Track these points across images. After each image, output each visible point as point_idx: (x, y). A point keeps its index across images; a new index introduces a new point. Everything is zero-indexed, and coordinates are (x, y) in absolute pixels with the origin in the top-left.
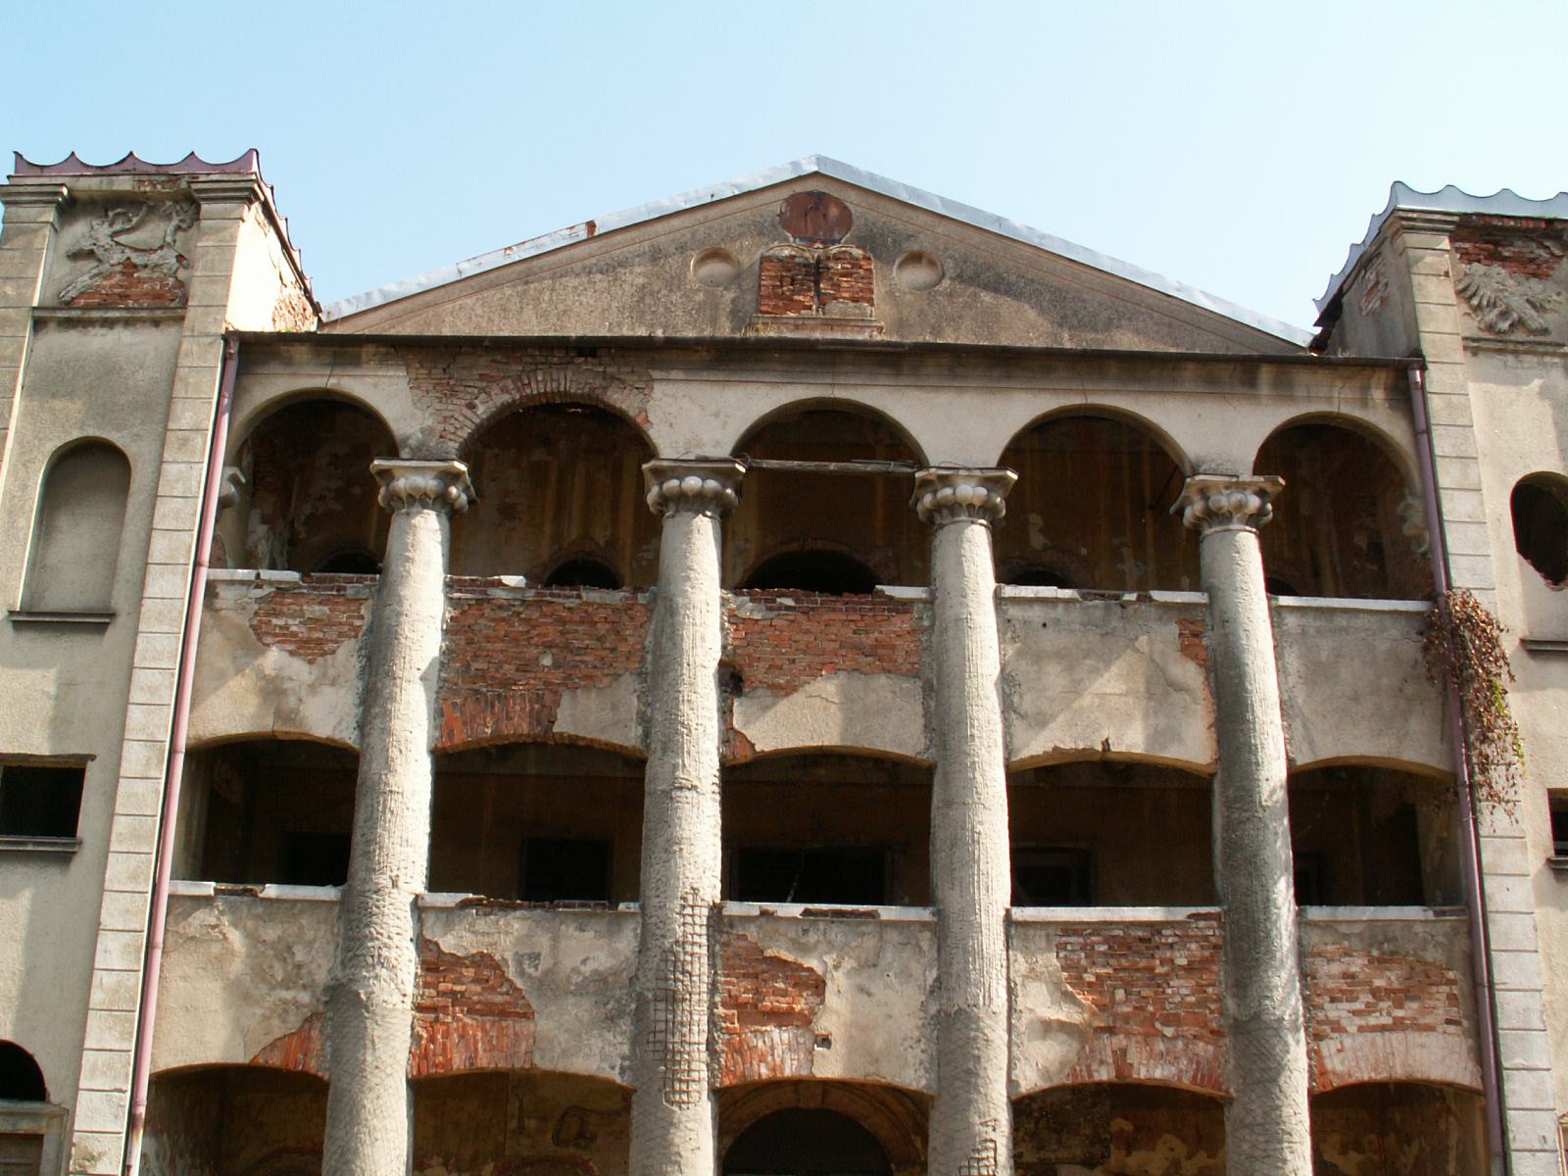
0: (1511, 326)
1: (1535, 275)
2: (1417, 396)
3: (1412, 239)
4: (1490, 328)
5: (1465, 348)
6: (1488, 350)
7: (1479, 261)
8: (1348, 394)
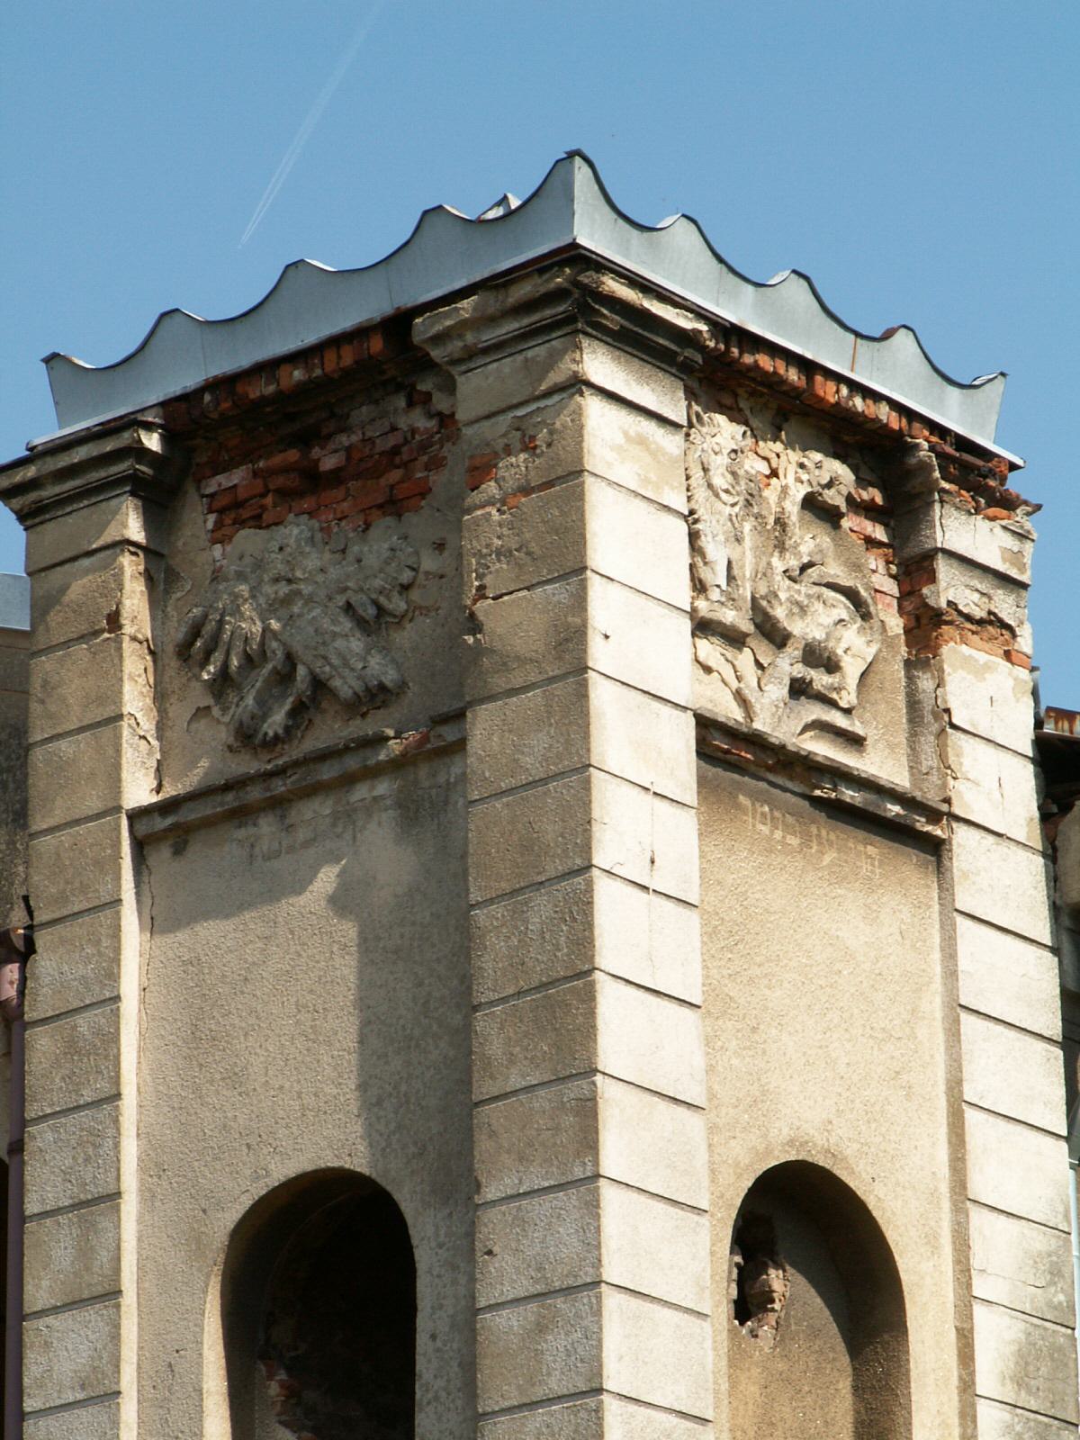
6: (208, 823)
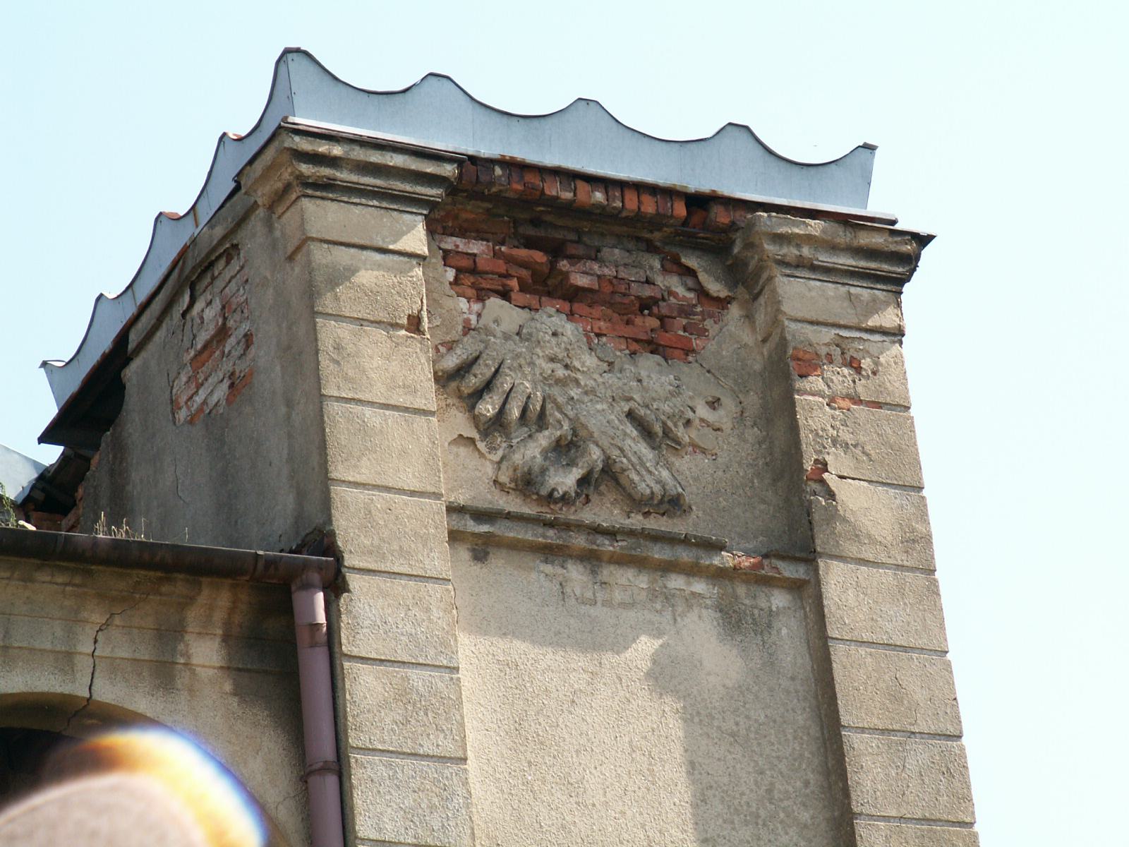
0: (583, 482)
1: (654, 347)
2: (314, 664)
3: (325, 216)
4: (526, 483)
5: (455, 537)
6: (515, 546)
7: (505, 295)
8: (119, 646)
